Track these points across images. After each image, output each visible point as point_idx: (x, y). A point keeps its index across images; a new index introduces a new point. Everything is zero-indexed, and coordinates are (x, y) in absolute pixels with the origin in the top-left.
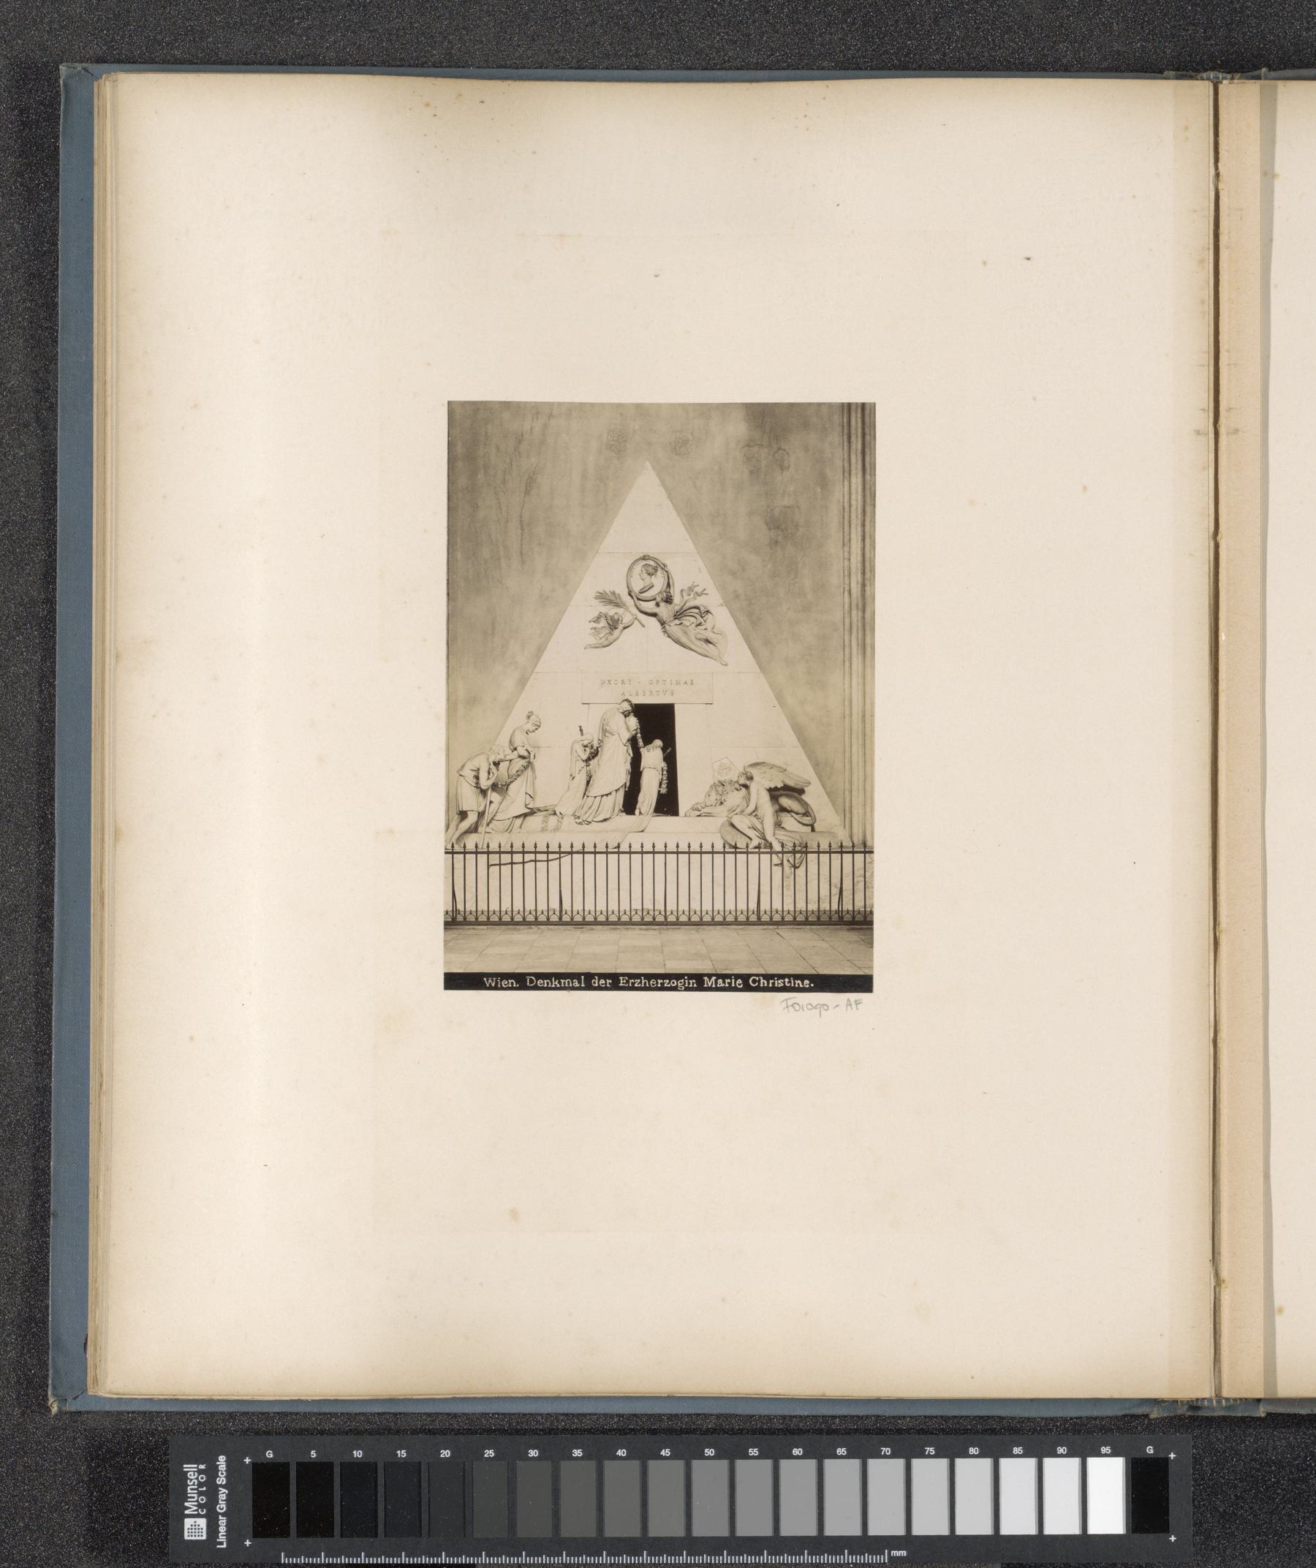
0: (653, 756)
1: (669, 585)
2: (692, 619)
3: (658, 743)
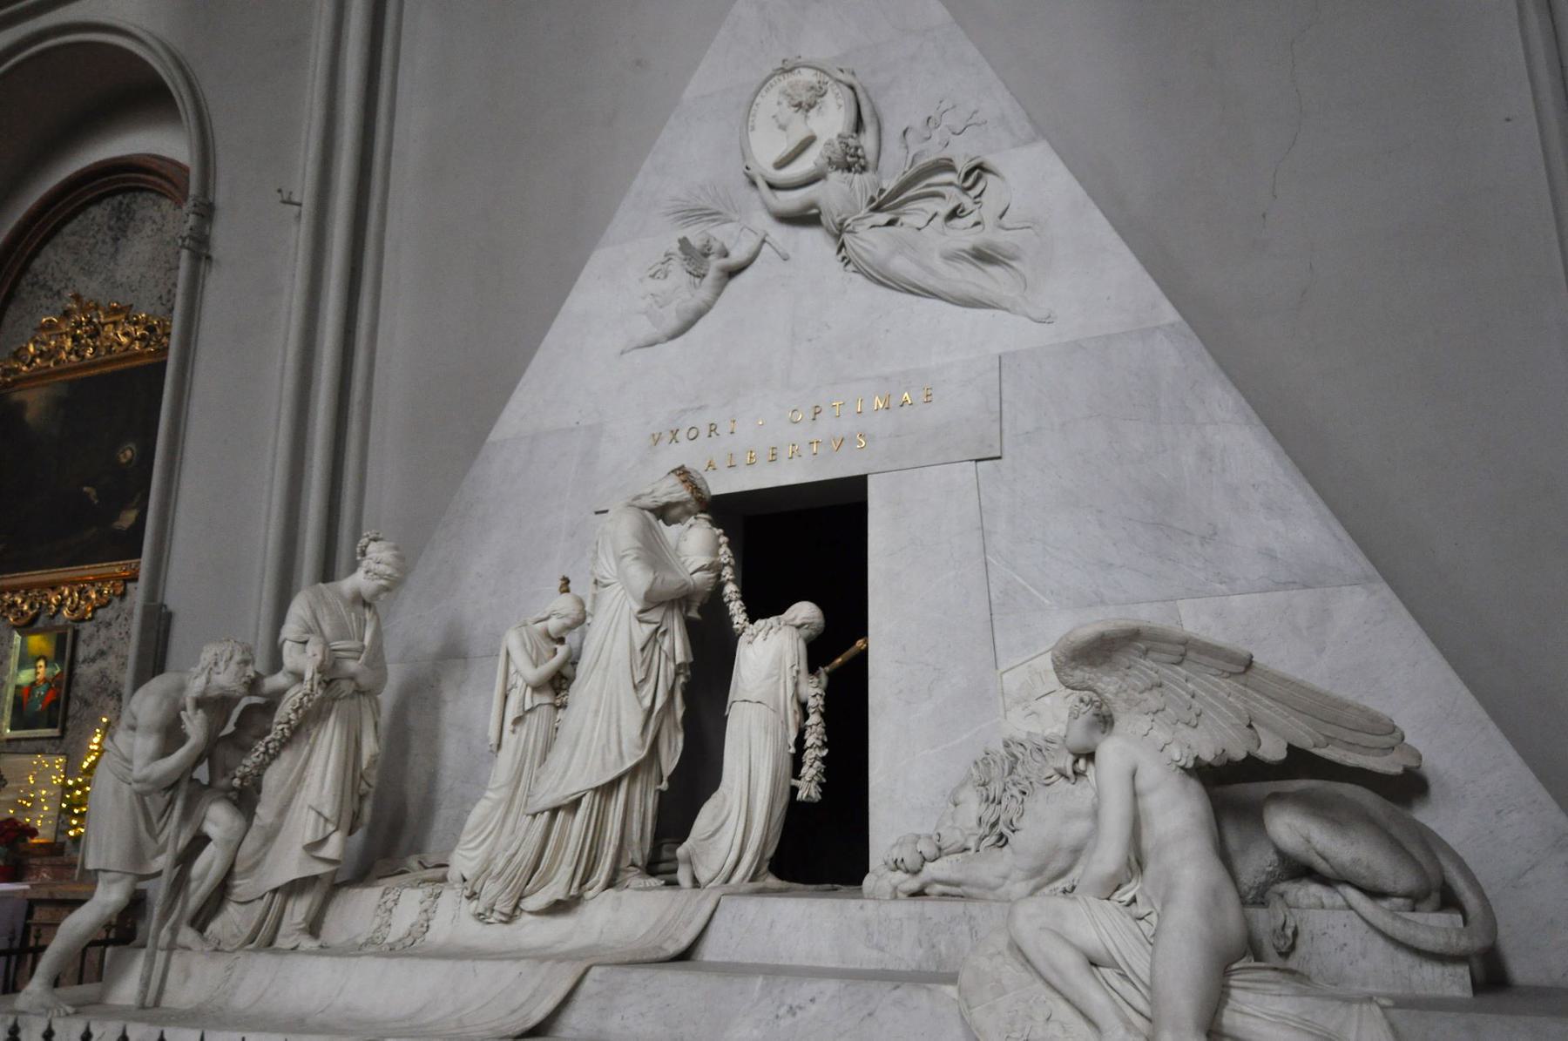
0: (770, 655)
1: (859, 125)
2: (931, 206)
3: (805, 611)
